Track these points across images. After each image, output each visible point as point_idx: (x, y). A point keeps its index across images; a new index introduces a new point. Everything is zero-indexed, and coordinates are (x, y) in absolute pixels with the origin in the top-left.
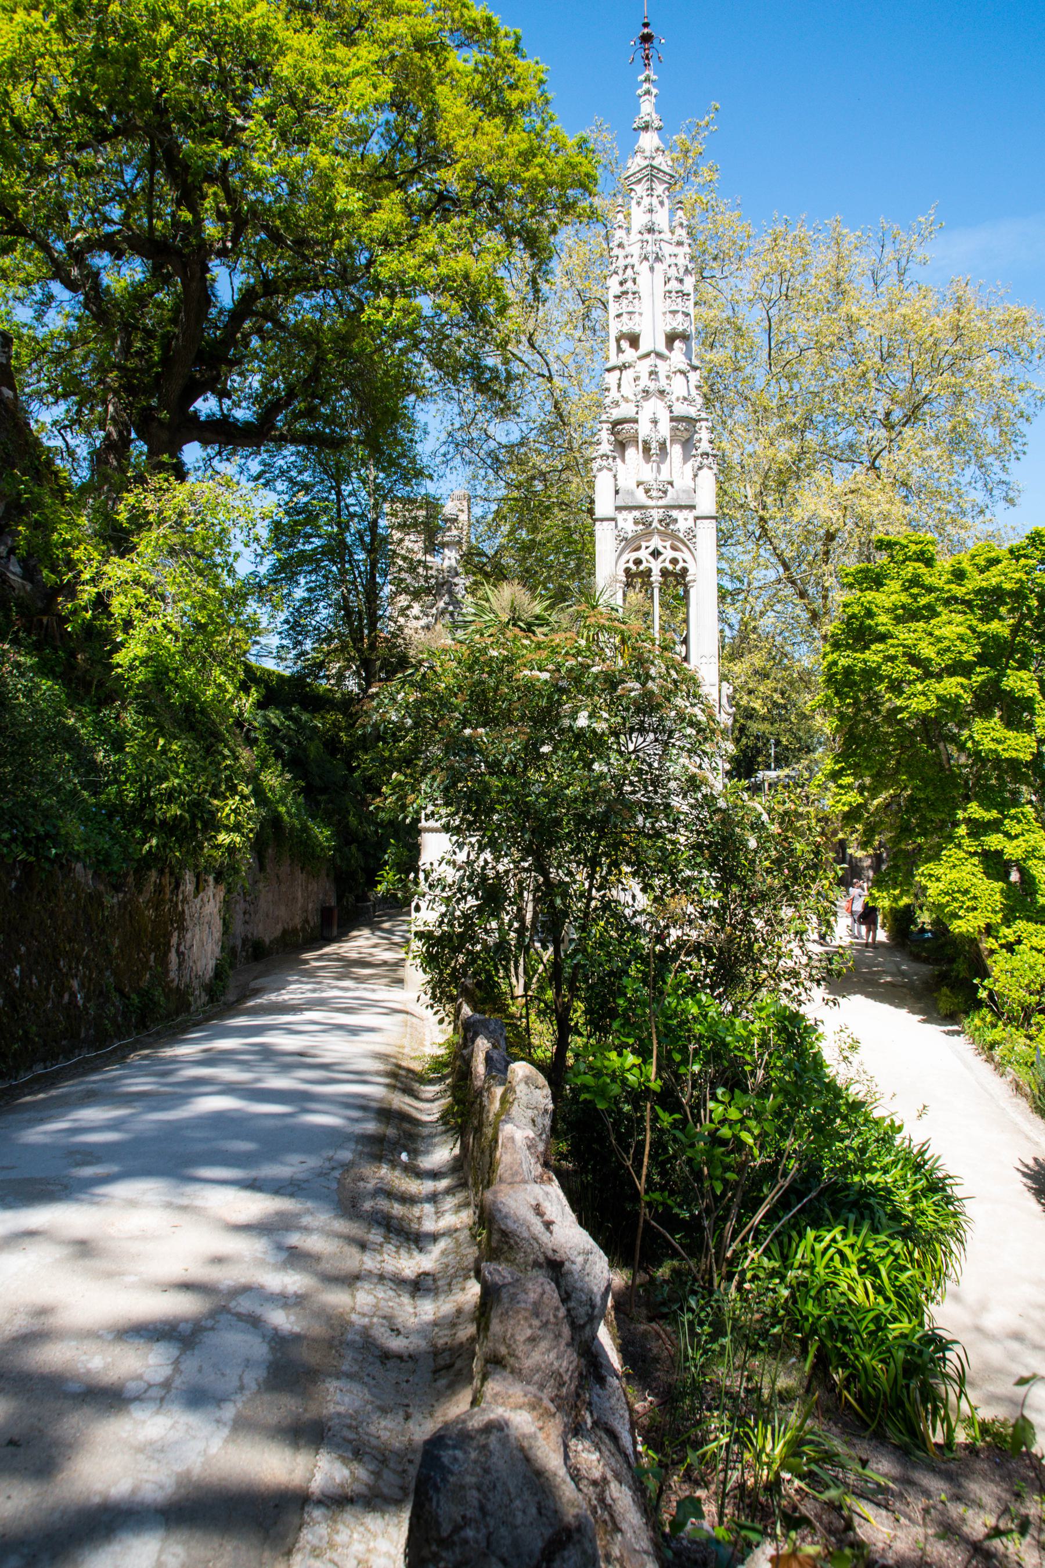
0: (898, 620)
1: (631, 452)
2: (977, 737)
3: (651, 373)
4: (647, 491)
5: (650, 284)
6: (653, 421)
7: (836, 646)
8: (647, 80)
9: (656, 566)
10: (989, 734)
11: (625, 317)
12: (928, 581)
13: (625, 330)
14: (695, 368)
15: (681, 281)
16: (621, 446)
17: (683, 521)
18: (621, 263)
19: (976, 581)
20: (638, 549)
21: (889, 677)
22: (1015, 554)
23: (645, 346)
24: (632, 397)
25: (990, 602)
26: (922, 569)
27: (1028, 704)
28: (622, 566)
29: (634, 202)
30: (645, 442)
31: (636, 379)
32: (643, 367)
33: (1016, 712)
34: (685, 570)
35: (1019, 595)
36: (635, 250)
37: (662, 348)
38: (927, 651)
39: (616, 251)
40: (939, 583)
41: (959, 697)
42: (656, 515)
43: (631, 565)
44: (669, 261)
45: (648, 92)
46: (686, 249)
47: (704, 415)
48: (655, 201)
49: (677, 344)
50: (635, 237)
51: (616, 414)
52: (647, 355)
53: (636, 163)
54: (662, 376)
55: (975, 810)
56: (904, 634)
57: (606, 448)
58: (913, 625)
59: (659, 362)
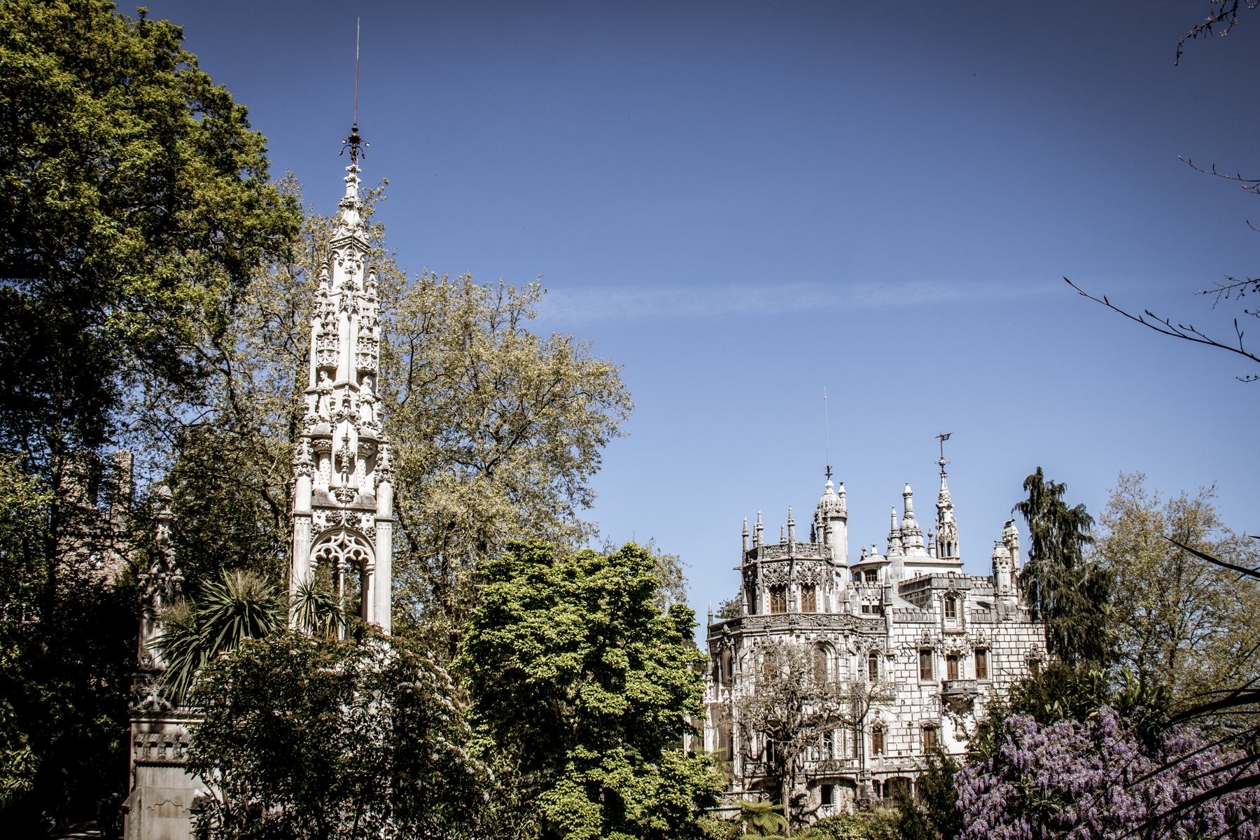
0: (527, 607)
1: (324, 462)
2: (584, 697)
3: (345, 401)
4: (338, 495)
5: (347, 329)
6: (344, 438)
7: (480, 626)
8: (353, 170)
9: (342, 557)
10: (593, 695)
11: (326, 354)
12: (550, 579)
13: (325, 363)
14: (378, 400)
15: (371, 330)
16: (317, 456)
17: (366, 522)
18: (324, 309)
19: (583, 582)
20: (329, 540)
21: (520, 651)
22: (613, 562)
23: (341, 378)
24: (328, 418)
25: (593, 595)
26: (546, 570)
27: (620, 673)
28: (313, 558)
29: (336, 263)
30: (338, 456)
31: (333, 404)
32: (339, 395)
33: (611, 679)
34: (365, 560)
35: (616, 594)
36: (336, 300)
37: (354, 382)
38: (551, 633)
39: (320, 299)
40: (558, 579)
41: (573, 668)
42: (344, 515)
43: (322, 553)
44: (362, 313)
45: (353, 180)
46: (377, 306)
47: (385, 439)
48: (354, 265)
49: (366, 379)
50: (335, 290)
51: (313, 429)
52: (342, 386)
53: (341, 233)
54: (353, 404)
55: (581, 751)
56: (532, 619)
57: (306, 457)
58: (538, 612)
59: (351, 393)
